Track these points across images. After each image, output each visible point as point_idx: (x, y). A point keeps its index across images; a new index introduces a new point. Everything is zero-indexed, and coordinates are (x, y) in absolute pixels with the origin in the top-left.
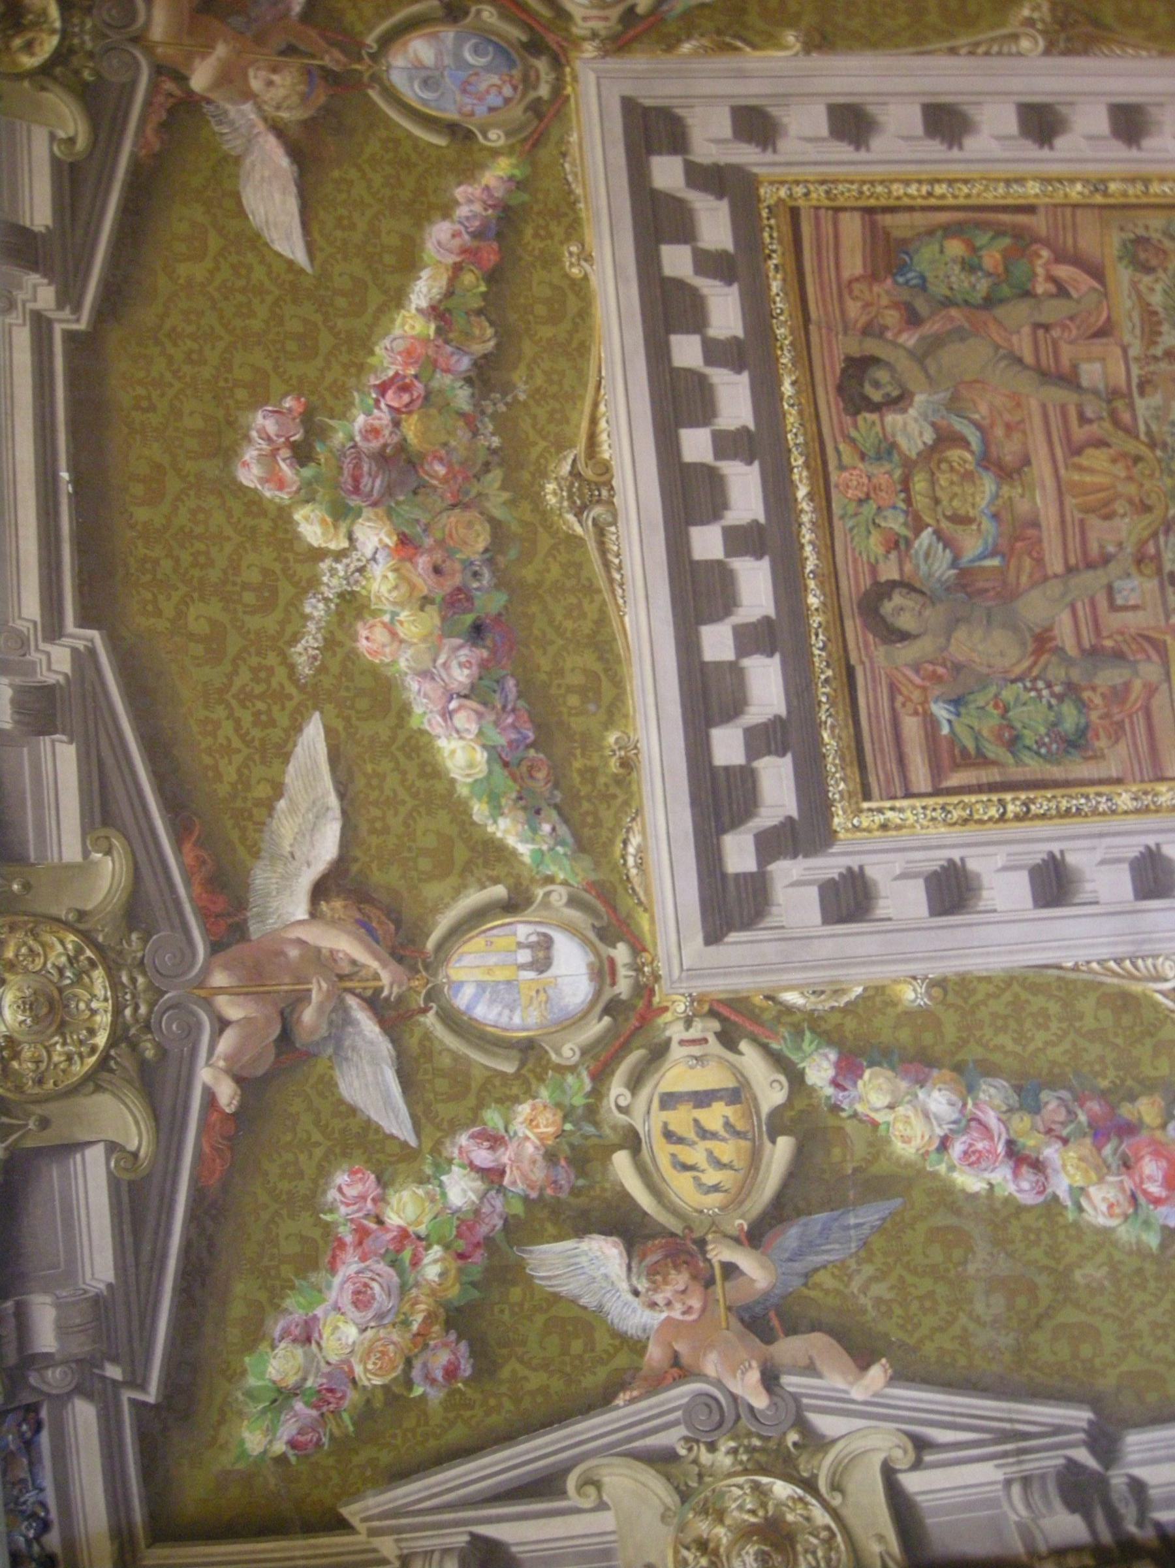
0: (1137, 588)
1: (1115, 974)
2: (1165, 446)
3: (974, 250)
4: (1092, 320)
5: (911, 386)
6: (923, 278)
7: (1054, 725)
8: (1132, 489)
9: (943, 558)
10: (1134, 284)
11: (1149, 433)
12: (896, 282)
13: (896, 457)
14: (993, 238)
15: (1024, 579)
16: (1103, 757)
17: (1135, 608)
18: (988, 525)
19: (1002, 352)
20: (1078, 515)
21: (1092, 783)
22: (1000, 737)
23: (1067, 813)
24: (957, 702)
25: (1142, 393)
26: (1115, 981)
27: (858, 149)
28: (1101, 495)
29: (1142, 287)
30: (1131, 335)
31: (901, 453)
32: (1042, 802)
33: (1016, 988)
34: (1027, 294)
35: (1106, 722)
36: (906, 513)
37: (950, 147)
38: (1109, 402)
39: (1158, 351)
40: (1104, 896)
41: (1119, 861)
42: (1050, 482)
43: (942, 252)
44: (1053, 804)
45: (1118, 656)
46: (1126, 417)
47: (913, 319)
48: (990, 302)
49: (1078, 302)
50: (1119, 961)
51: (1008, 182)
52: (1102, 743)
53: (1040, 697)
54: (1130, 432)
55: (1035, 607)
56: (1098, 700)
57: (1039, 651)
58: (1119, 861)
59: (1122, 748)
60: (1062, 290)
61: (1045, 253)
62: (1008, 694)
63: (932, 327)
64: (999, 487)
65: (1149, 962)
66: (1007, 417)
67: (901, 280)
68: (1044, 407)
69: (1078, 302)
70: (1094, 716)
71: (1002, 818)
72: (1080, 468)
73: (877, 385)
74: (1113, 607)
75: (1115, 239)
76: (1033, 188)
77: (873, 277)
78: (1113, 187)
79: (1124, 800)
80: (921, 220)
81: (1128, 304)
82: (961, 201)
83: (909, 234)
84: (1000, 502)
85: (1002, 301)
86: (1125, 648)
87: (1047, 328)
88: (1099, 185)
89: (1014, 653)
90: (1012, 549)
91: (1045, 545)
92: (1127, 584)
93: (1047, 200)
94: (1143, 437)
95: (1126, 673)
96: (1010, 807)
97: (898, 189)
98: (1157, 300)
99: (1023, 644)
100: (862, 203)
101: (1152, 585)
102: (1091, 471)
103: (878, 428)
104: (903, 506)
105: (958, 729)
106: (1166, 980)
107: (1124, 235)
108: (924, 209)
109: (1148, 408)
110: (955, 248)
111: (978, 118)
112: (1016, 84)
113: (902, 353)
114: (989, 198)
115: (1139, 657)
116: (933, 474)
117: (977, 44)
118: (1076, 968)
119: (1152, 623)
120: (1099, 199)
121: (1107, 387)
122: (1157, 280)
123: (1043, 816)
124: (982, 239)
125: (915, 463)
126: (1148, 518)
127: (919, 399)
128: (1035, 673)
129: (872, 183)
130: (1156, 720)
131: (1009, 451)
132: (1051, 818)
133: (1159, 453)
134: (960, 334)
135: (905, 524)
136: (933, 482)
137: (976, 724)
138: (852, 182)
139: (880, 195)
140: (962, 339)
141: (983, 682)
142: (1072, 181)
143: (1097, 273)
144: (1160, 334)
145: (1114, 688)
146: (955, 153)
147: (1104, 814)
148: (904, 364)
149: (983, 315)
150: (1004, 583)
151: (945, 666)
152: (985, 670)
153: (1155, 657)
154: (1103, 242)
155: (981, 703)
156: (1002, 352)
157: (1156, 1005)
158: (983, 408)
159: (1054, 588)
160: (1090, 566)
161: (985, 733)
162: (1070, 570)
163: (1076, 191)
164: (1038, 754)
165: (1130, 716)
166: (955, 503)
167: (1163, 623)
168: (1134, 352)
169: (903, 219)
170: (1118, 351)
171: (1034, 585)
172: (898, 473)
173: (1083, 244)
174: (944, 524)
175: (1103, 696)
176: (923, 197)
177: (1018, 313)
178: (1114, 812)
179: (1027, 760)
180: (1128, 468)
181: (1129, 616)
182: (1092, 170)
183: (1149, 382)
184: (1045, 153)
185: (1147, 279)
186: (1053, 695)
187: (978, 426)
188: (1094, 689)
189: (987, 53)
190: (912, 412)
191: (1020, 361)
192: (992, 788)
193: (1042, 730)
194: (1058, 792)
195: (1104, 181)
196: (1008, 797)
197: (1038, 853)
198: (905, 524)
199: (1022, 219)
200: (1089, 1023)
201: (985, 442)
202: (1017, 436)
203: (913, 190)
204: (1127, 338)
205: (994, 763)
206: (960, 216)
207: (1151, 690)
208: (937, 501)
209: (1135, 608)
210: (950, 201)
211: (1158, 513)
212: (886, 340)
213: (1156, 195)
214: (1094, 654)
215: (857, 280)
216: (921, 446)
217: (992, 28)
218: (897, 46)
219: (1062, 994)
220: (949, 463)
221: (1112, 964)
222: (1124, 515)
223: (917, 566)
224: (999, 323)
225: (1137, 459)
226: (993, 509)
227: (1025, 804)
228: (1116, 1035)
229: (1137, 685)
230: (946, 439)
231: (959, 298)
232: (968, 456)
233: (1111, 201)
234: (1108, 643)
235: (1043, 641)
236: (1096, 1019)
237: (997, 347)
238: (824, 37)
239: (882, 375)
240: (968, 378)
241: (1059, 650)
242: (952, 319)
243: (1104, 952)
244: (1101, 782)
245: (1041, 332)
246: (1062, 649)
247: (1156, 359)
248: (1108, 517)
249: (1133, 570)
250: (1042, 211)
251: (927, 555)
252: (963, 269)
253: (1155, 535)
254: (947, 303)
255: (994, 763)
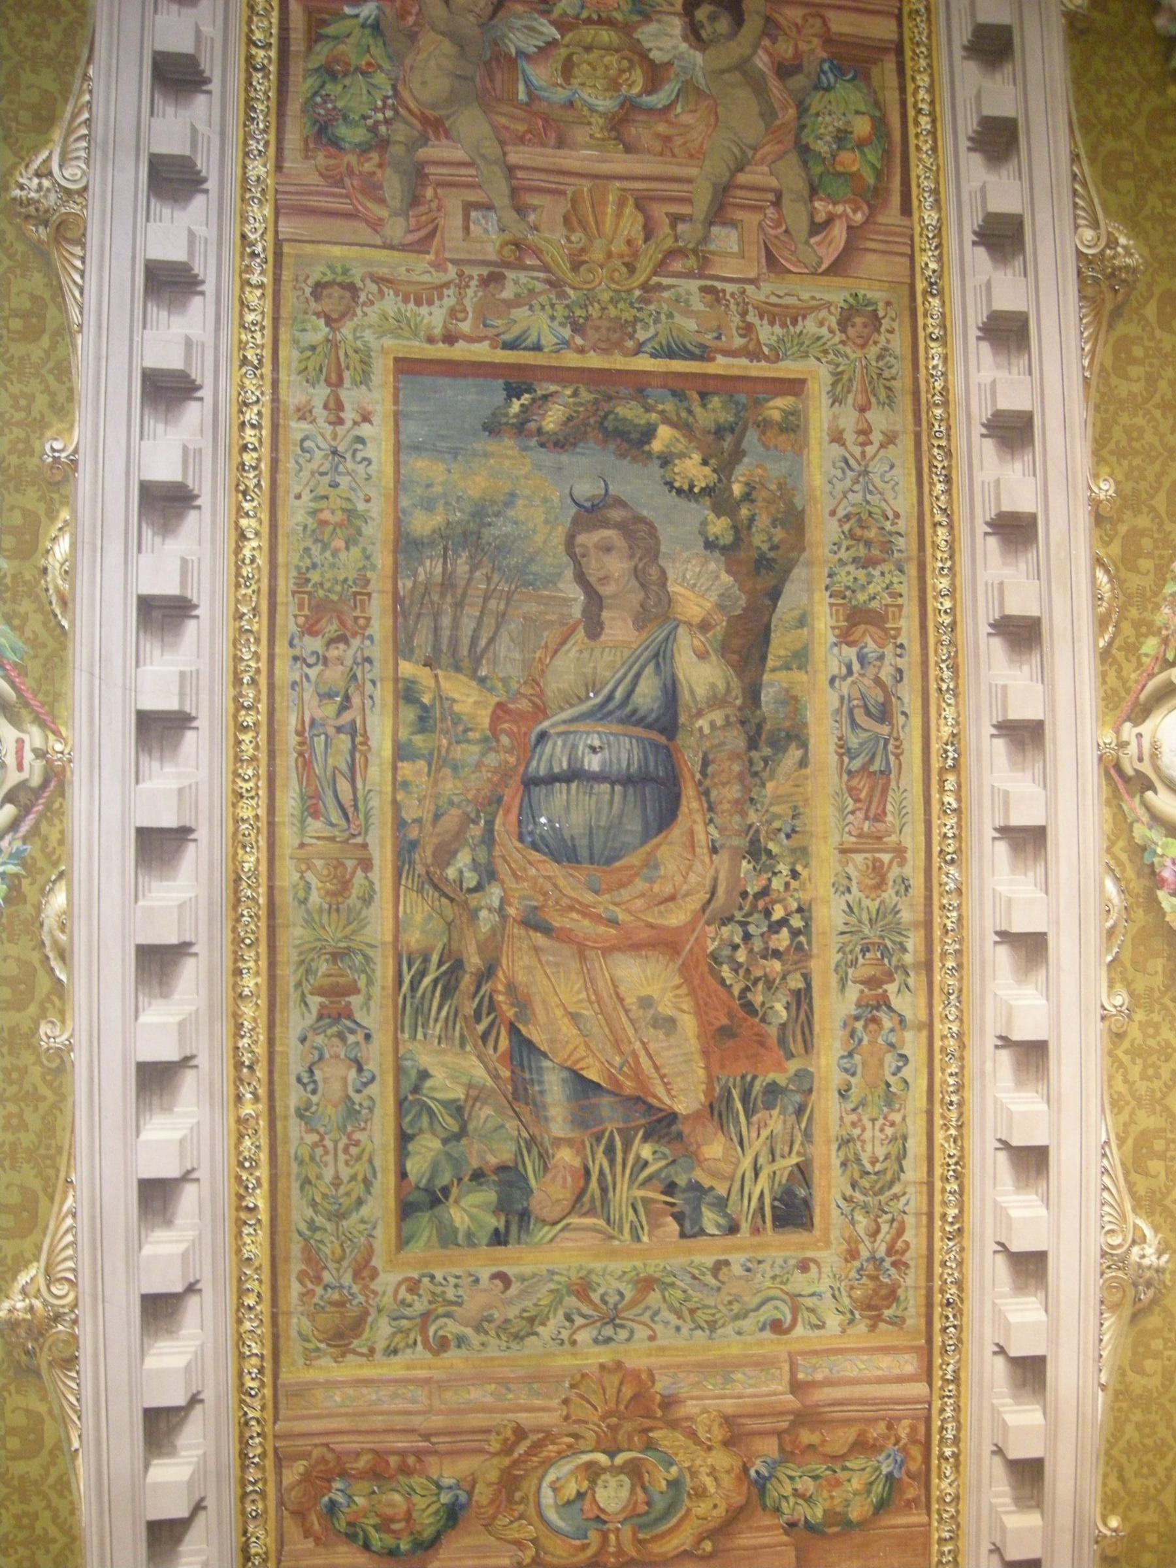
0: (489, 236)
1: (74, 116)
2: (648, 302)
3: (861, 145)
4: (787, 254)
5: (711, 51)
6: (828, 89)
7: (345, 118)
8: (597, 255)
9: (530, 45)
10: (828, 305)
11: (659, 287)
12: (823, 61)
13: (636, 18)
14: (873, 166)
15: (504, 121)
16: (307, 158)
17: (466, 229)
18: (561, 95)
19: (750, 153)
20: (570, 191)
21: (280, 140)
22: (337, 60)
23: (249, 107)
24: (376, 28)
25: (703, 289)
26: (68, 115)
27: (965, 48)
28: (591, 219)
29: (824, 313)
30: (766, 291)
31: (640, 23)
32: (264, 85)
33: (74, 14)
34: (813, 191)
35: (343, 170)
36: (577, 17)
37: (970, 139)
38: (695, 252)
39: (752, 318)
40: (157, 122)
41: (194, 145)
42: (605, 168)
43: (857, 112)
44: (260, 95)
45: (415, 200)
46: (677, 265)
47: (784, 71)
48: (804, 151)
49: (807, 243)
50: (88, 123)
51: (936, 192)
52: (321, 159)
53: (376, 110)
54: (660, 268)
55: (472, 126)
56: (368, 167)
57: (425, 120)
58: (194, 145)
59: (314, 179)
60: (817, 228)
61: (859, 217)
62: (380, 78)
63: (774, 85)
64: (602, 115)
65: (83, 154)
66: (678, 141)
67: (826, 67)
68: (689, 181)
69: (807, 243)
70: (352, 159)
71: (251, 42)
72: (621, 204)
73: (713, 18)
74: (468, 207)
75: (877, 295)
76: (930, 217)
77: (828, 40)
78: (935, 302)
79: (258, 169)
80: (891, 97)
81: (805, 296)
82: (913, 141)
83: (875, 83)
84: (586, 112)
85: (805, 163)
86: (423, 209)
87: (777, 203)
88: (935, 288)
89: (426, 96)
90: (535, 114)
91: (539, 150)
92: (492, 227)
93: (917, 230)
94: (655, 280)
95: (396, 204)
96: (262, 53)
97: (923, 80)
98: (810, 326)
99: (434, 106)
100: (907, 45)
101: (492, 254)
102: (619, 215)
103: (666, 8)
104: (585, 15)
105: (348, 23)
106: (61, 167)
107: (881, 305)
108: (903, 103)
109: (688, 293)
110: (862, 127)
111: (1004, 173)
112: (1043, 218)
113: (748, 51)
114: (916, 170)
115: (412, 221)
116: (617, 51)
117: (1084, 185)
118: (86, 77)
119: (448, 244)
120: (920, 285)
121: (713, 253)
122: (831, 331)
123: (249, 82)
124: (872, 155)
125: (630, 36)
126: (566, 266)
127: (698, 57)
128: (402, 111)
129: (929, 56)
130: (340, 223)
131: (639, 131)
132: (247, 91)
133: (637, 293)
134: (768, 114)
135: (564, 14)
136: (608, 49)
137: (351, 40)
138: (929, 37)
139: (916, 63)
140: (762, 115)
141: (396, 58)
142: (940, 259)
143: (837, 268)
144: (772, 323)
145: (381, 187)
146: (964, 144)
147: (246, 144)
148: (736, 49)
149: (789, 139)
150: (499, 100)
151: (416, 24)
152: (408, 61)
153: (410, 238)
154: (873, 278)
155: (373, 50)
156: (750, 153)
157: (36, 149)
158: (687, 119)
159: (491, 148)
160: (514, 192)
161: (342, 47)
162: (511, 170)
163: (927, 260)
164: (315, 94)
165: (347, 196)
166: (585, 67)
167: (448, 255)
168: (750, 289)
169: (892, 80)
170: (752, 275)
171: (495, 128)
172: (618, 16)
173: (870, 258)
174: (563, 52)
175: (373, 174)
176: (915, 105)
177: (792, 177)
178: (246, 154)
179: (310, 81)
180: (621, 256)
181: (459, 222)
182: (953, 282)
183: (718, 300)
184: (969, 237)
185: (833, 321)
186: (377, 123)
187: (669, 108)
188: (380, 166)
189: (1075, 193)
190: (684, 46)
191: (741, 169)
192: (284, 41)
193: (340, 104)
194: (273, 104)
195: (940, 294)
196: (273, 54)
197: (211, 66)
198: (564, 14)
199: (896, 200)
200: (27, 77)
201: (650, 111)
202: (658, 145)
203: (922, 94)
204: (766, 287)
205: (310, 49)
206: (897, 136)
207: (376, 225)
208: (588, 49)
209: (466, 229)
210: (912, 131)
211: (570, 275)
212: (760, 38)
213: (927, 348)
214: (418, 175)
215: (825, 23)
216: (647, 45)
217: (1104, 203)
218: (1077, 103)
219: (61, 57)
220: (629, 70)
221: (86, 115)
222: (569, 240)
223: (520, 18)
224: (780, 157)
225: (631, 268)
226: (579, 104)
227: (264, 68)
228: (11, 102)
229: (384, 213)
230: (656, 74)
231: (807, 120)
232: (636, 90)
233: (919, 299)
234: (429, 193)
235: (434, 126)
236: (29, 87)
237: (755, 149)
238: (1082, 32)
239: (723, 25)
240: (720, 110)
241: (425, 140)
242: (785, 108)
243: (99, 110)
244: (280, 150)
245: (771, 197)
246: (425, 144)
247: (744, 314)
248: (566, 220)
249: (507, 236)
250: (906, 222)
251: (532, 29)
252: (839, 130)
253: (546, 268)
254: (802, 108)
255: (310, 49)
